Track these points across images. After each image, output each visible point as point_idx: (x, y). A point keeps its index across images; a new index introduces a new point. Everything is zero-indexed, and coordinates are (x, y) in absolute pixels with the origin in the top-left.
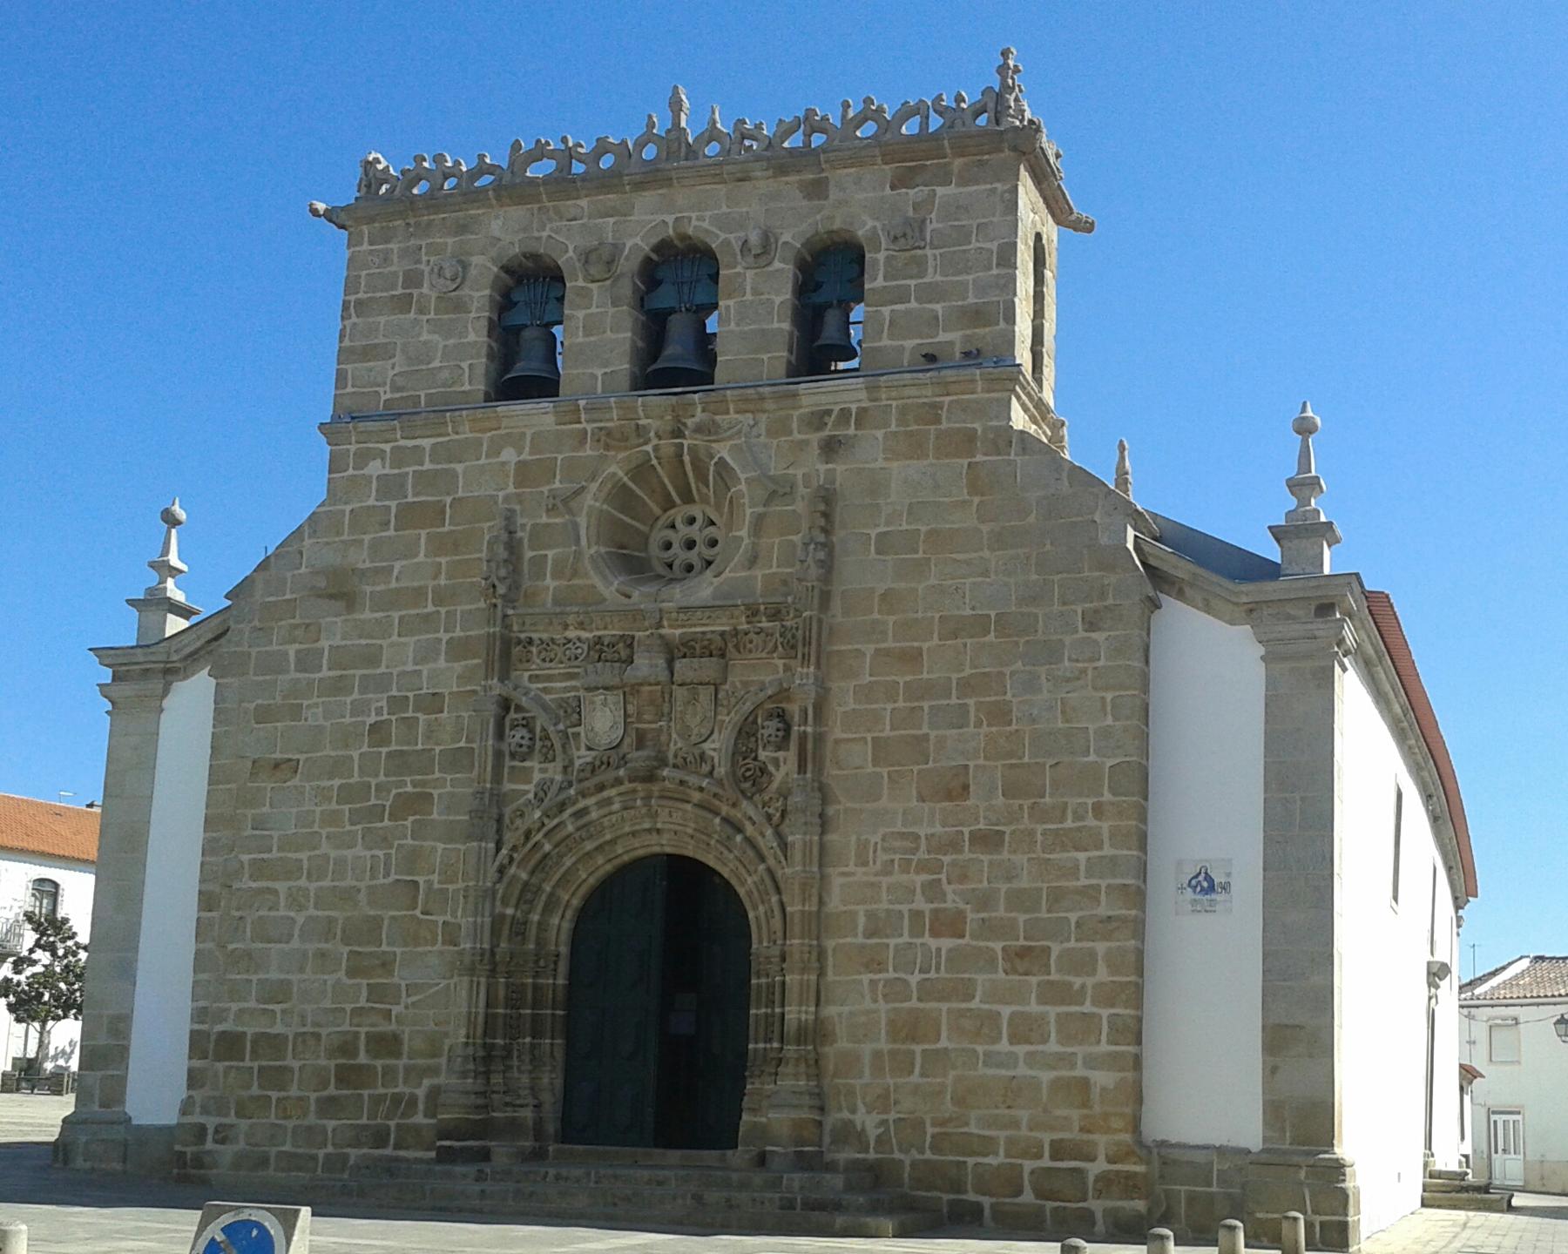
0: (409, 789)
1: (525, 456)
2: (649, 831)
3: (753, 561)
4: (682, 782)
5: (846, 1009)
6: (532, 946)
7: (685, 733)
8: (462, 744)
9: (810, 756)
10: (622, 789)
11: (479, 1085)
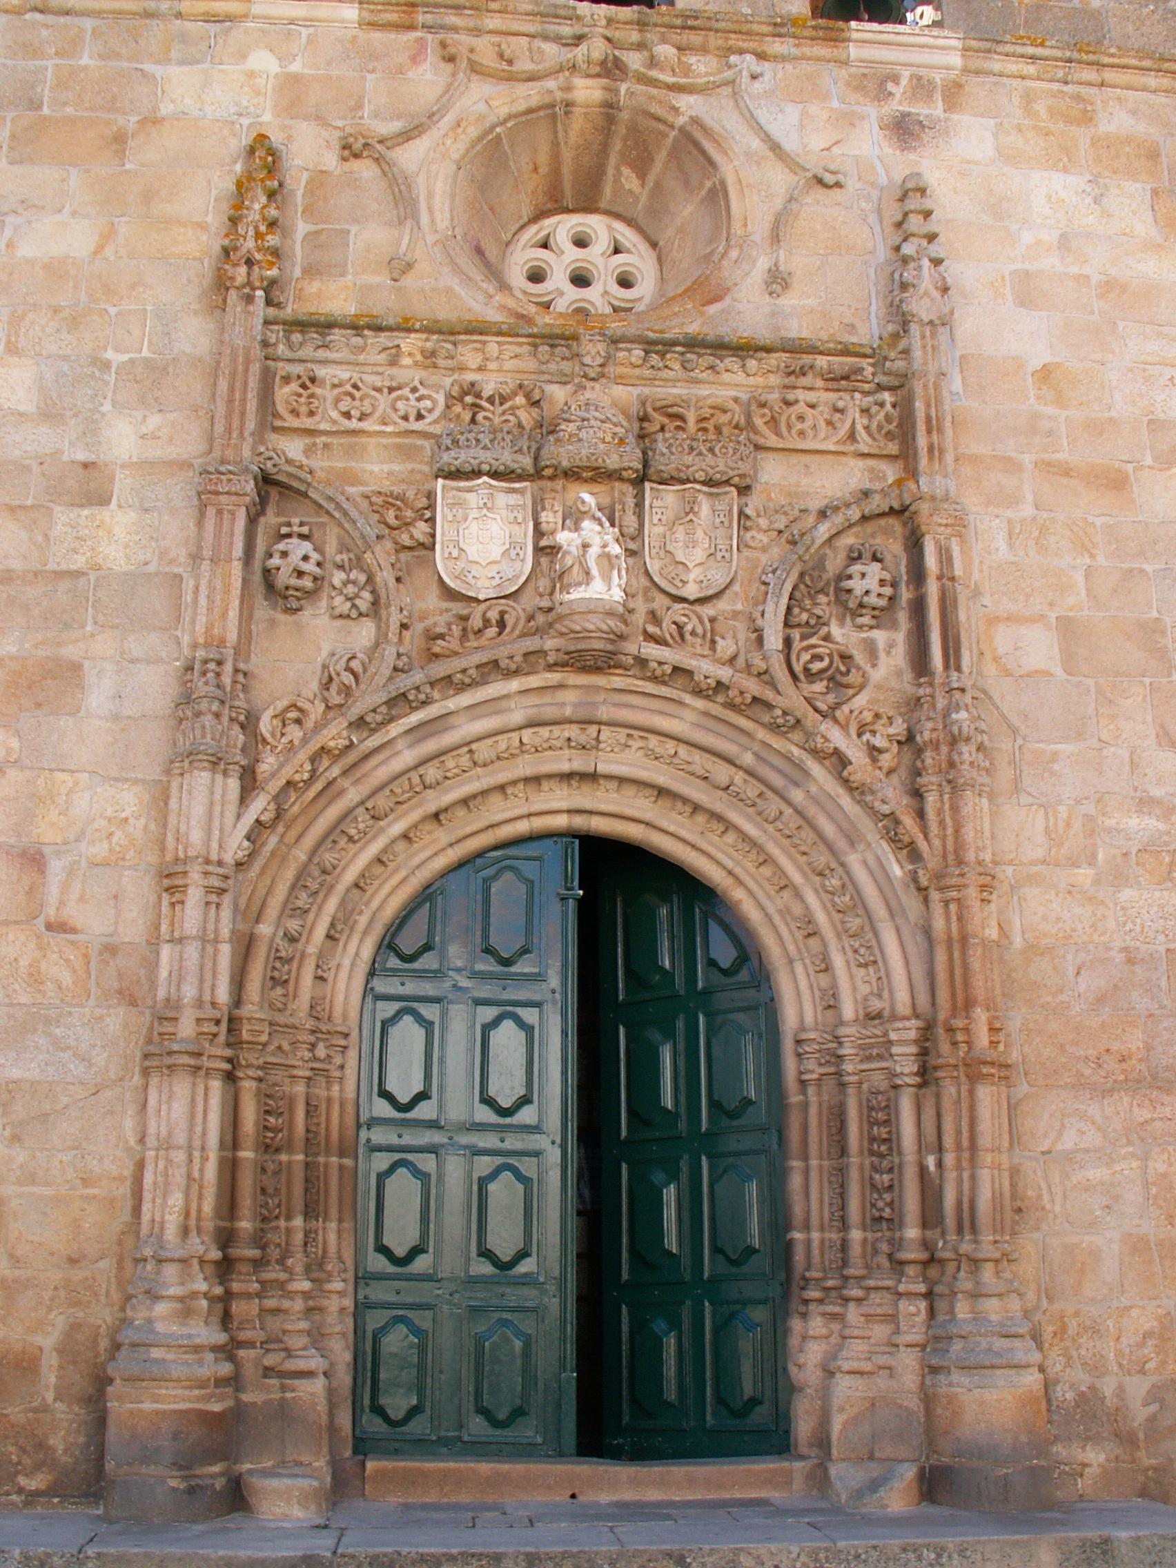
1: (296, 67)
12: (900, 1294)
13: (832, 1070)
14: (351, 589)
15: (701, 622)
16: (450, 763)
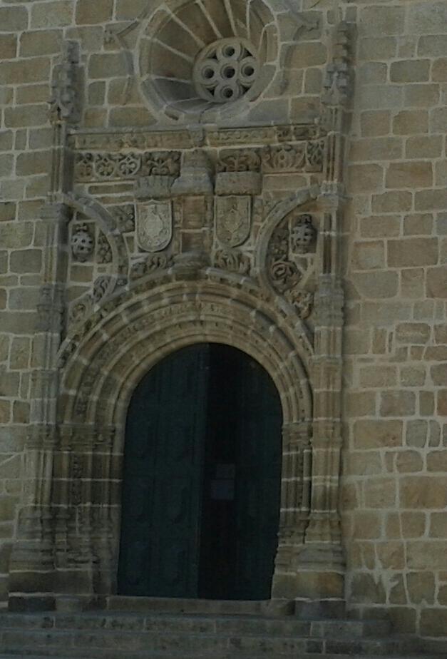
2: (194, 322)
3: (284, 87)
4: (222, 280)
5: (365, 478)
6: (91, 423)
7: (225, 238)
8: (31, 247)
9: (334, 257)
10: (170, 286)
11: (46, 543)
15: (234, 259)
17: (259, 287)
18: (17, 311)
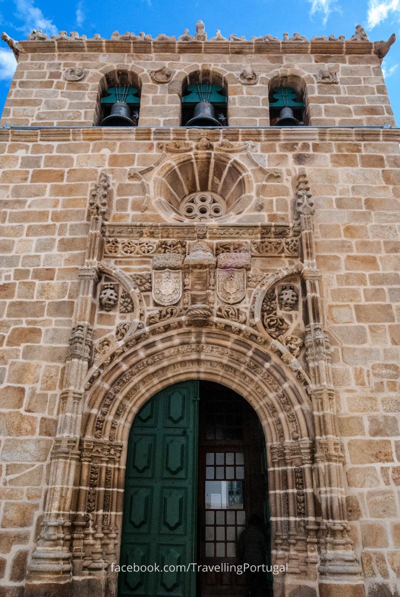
0: (24, 325)
1: (116, 152)
8: (66, 299)
10: (181, 330)
12: (308, 543)
13: (282, 458)
14: (126, 304)
15: (234, 311)
16: (156, 357)
17: (258, 331)
18: (50, 345)
